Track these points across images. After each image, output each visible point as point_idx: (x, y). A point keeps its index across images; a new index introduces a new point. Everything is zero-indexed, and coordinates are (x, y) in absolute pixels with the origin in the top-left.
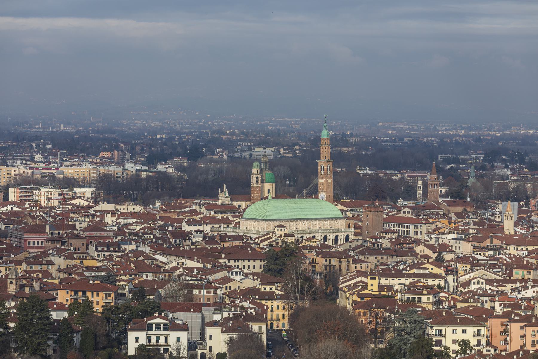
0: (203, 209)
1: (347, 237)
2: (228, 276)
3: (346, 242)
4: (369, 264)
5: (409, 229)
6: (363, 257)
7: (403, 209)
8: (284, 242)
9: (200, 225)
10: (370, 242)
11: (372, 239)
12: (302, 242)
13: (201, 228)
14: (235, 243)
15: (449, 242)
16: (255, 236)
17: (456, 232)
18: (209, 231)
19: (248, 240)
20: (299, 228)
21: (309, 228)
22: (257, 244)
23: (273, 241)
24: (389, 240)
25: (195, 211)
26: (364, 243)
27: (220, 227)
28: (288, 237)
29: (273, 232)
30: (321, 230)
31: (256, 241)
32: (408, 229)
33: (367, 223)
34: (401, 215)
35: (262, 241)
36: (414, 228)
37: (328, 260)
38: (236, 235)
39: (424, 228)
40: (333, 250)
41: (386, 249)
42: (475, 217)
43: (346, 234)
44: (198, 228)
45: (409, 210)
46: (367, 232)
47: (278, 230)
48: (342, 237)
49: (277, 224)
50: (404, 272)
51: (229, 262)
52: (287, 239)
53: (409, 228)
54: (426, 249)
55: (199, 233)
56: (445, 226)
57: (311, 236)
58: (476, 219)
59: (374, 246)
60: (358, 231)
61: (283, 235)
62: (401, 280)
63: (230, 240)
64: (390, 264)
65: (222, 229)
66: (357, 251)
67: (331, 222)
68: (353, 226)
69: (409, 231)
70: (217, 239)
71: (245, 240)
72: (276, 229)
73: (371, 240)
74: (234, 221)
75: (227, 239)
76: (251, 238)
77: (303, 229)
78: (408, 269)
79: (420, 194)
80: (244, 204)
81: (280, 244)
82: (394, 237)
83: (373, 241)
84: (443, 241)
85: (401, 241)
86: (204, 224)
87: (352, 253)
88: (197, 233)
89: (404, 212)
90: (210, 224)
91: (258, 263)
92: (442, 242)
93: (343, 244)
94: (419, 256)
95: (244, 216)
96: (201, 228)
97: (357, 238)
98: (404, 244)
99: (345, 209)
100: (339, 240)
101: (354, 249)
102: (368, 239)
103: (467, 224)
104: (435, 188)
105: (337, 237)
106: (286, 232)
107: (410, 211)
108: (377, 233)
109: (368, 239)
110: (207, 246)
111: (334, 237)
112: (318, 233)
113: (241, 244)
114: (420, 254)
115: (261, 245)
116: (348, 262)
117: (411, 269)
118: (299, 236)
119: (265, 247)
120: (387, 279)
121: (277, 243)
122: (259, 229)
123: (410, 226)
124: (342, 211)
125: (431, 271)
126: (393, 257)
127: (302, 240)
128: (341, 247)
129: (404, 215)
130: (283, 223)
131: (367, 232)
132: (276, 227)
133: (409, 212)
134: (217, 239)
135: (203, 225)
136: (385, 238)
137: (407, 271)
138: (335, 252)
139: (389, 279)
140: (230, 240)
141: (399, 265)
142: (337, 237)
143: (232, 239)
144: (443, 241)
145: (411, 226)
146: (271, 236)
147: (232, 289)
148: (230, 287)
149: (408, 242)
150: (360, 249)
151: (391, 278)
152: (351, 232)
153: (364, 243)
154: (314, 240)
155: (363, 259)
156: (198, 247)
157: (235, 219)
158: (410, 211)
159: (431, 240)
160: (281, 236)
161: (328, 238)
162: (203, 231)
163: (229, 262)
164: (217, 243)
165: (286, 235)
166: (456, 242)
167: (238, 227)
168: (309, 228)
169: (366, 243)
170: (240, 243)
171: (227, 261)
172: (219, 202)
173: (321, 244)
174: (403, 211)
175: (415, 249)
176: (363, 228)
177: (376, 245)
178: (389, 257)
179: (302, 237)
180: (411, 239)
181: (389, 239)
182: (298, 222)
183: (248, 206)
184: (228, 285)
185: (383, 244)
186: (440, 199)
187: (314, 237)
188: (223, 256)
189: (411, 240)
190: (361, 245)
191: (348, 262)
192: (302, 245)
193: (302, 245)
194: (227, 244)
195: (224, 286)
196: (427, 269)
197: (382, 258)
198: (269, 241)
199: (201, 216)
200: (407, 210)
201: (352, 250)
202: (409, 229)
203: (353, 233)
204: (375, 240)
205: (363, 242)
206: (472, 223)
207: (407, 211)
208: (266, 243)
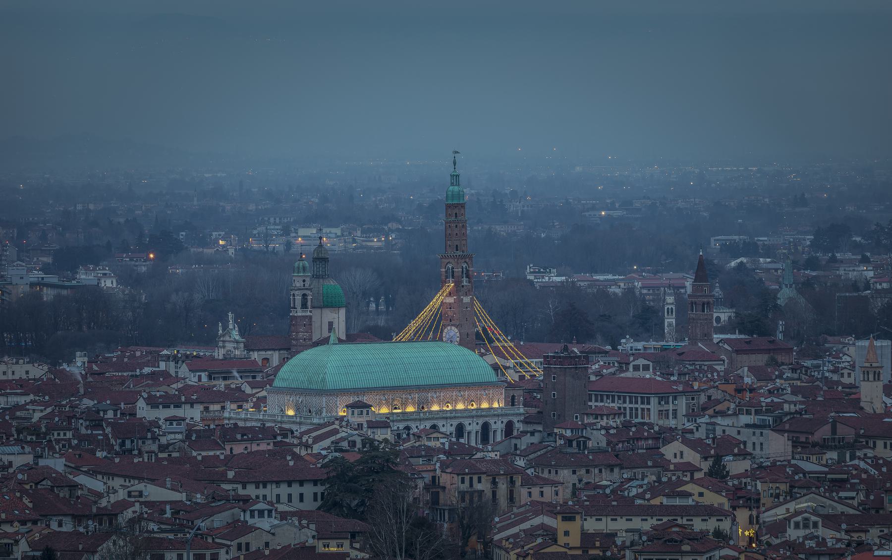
0: (184, 371)
2: (242, 519)
4: (560, 488)
5: (648, 407)
6: (546, 471)
7: (634, 361)
8: (369, 442)
9: (178, 406)
10: (562, 436)
11: (566, 429)
13: (179, 412)
15: (739, 433)
16: (304, 428)
17: (753, 410)
18: (197, 416)
19: (285, 436)
22: (307, 446)
23: (343, 439)
24: (603, 432)
25: (166, 374)
27: (223, 408)
28: (375, 430)
31: (304, 440)
32: (645, 406)
33: (554, 394)
34: (630, 374)
35: (317, 440)
36: (659, 403)
37: (467, 478)
38: (259, 427)
39: (682, 404)
40: (479, 455)
41: (599, 451)
42: (796, 376)
43: (505, 420)
44: (172, 412)
45: (646, 362)
46: (554, 414)
48: (498, 426)
49: (351, 400)
50: (639, 502)
51: (244, 488)
53: (649, 403)
54: (687, 451)
55: (175, 423)
56: (728, 397)
57: (428, 424)
58: (799, 379)
59: (571, 445)
61: (365, 425)
62: (631, 520)
64: (607, 486)
65: (226, 415)
66: (532, 456)
69: (649, 410)
71: (279, 438)
74: (253, 395)
75: (239, 437)
76: (292, 432)
78: (648, 496)
80: (275, 358)
81: (359, 445)
82: (614, 425)
83: (568, 433)
84: (724, 431)
85: (631, 433)
86: (185, 403)
87: (521, 463)
88: (171, 424)
89: (636, 368)
90: (202, 403)
91: (309, 490)
92: (721, 434)
93: (500, 443)
94: (672, 467)
95: (277, 383)
96: (179, 412)
97: (530, 428)
98: (638, 439)
100: (491, 435)
101: (523, 455)
102: (556, 430)
103: (778, 390)
104: (703, 311)
105: (486, 427)
108: (577, 416)
109: (556, 430)
110: (194, 454)
111: (479, 428)
113: (271, 447)
114: (674, 461)
115: (316, 449)
117: (652, 498)
118: (401, 426)
119: (324, 453)
120: (601, 520)
123: (648, 398)
125: (700, 500)
126: (612, 470)
127: (408, 435)
129: (637, 374)
130: (366, 399)
131: (554, 414)
133: (646, 368)
135: (183, 405)
137: (645, 499)
139: (604, 519)
140: (245, 437)
141: (626, 486)
142: (486, 427)
143: (250, 436)
144: (724, 431)
145: (652, 400)
146: (338, 427)
147: (253, 548)
148: (247, 544)
149: (646, 434)
150: (539, 453)
151: (609, 518)
154: (435, 435)
155: (546, 475)
156: (175, 455)
157: (255, 391)
159: (697, 430)
160: (360, 426)
161: (468, 428)
162: (184, 419)
163: (244, 488)
164: (217, 446)
166: (754, 434)
169: (552, 439)
171: (240, 487)
172: (219, 354)
173: (451, 444)
175: (662, 450)
177: (574, 444)
178: (603, 470)
179: (408, 428)
180: (653, 428)
181: (602, 428)
183: (284, 361)
184: (243, 540)
185: (589, 439)
186: (715, 336)
187: (434, 427)
188: (231, 474)
189: (652, 431)
191: (512, 482)
192: (407, 445)
193: (407, 445)
194: (238, 449)
195: (234, 543)
196: (690, 495)
197: (588, 472)
198: (333, 438)
200: (641, 362)
202: (648, 407)
204: (572, 432)
206: (789, 389)
208: (327, 443)
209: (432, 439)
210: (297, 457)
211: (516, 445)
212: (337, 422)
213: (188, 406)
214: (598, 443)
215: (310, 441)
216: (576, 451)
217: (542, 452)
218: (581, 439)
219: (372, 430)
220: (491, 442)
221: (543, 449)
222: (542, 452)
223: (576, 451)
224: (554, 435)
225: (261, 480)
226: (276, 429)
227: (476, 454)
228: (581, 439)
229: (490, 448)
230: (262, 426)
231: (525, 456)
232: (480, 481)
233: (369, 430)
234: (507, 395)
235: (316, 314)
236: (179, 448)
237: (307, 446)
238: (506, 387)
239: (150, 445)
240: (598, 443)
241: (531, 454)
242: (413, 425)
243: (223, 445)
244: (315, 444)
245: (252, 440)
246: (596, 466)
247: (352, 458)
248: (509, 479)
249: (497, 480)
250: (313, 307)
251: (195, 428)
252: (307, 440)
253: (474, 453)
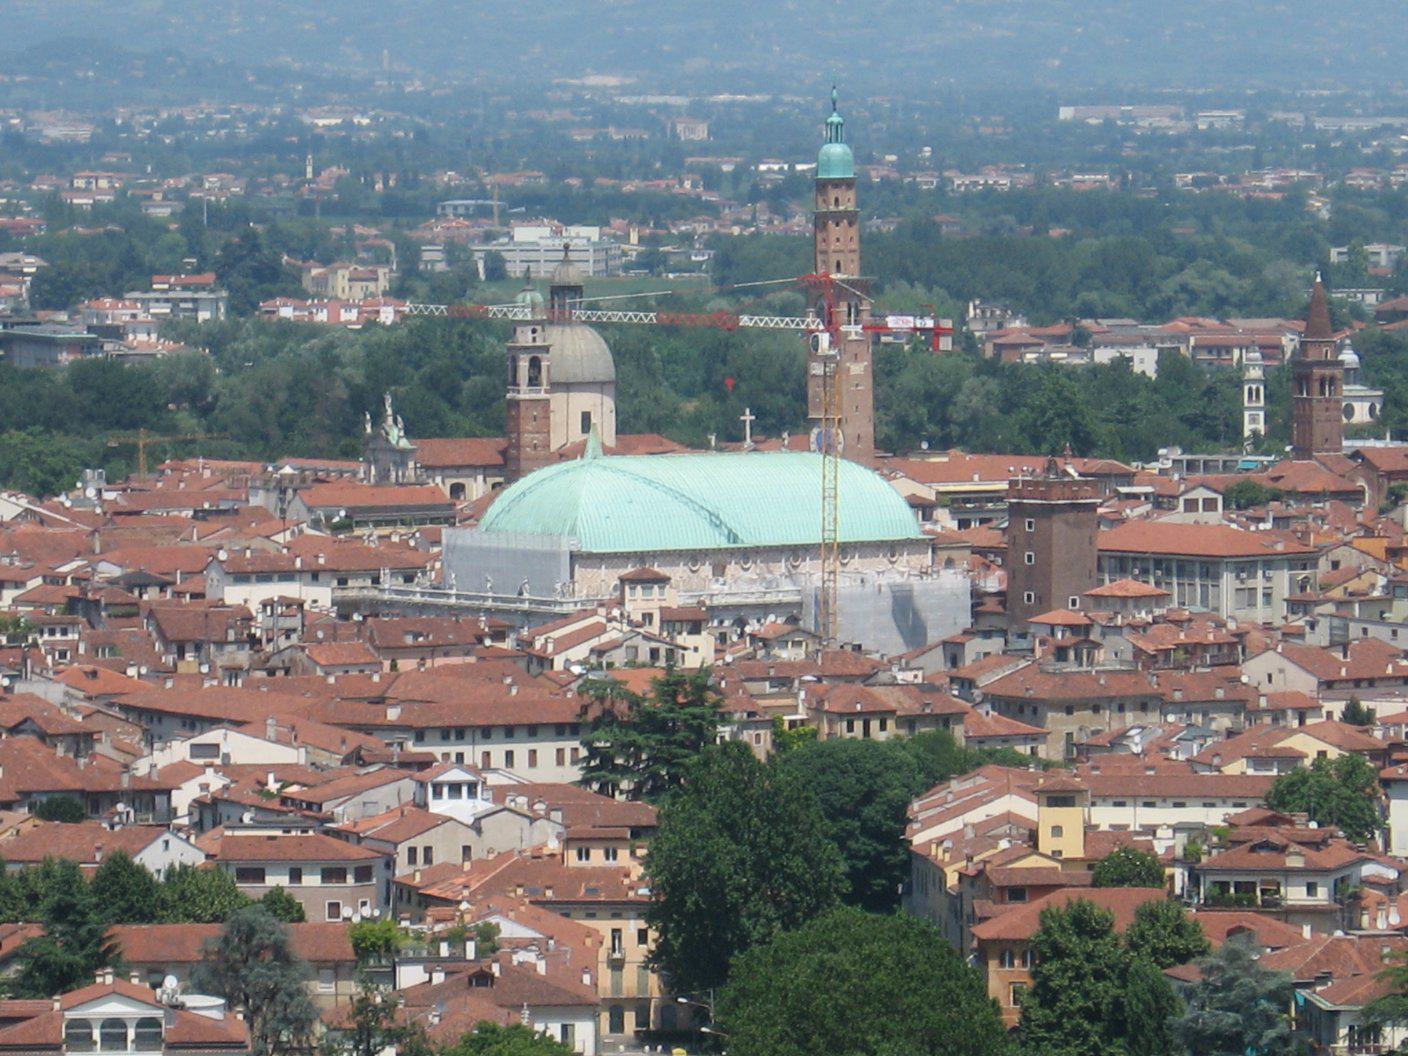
7: (1186, 492)
23: (615, 645)
33: (1030, 557)
45: (1211, 495)
46: (1029, 597)
79: (205, 787)
89: (1191, 506)
107: (1215, 501)
131: (1029, 597)
146: (604, 621)
148: (428, 850)
158: (1215, 501)
174: (1186, 501)
184: (420, 843)
198: (594, 642)
200: (1201, 494)
207: (1204, 500)
208: (580, 652)
212: (602, 611)
224: (1029, 637)
232: (883, 727)
235: (558, 400)
239: (231, 653)
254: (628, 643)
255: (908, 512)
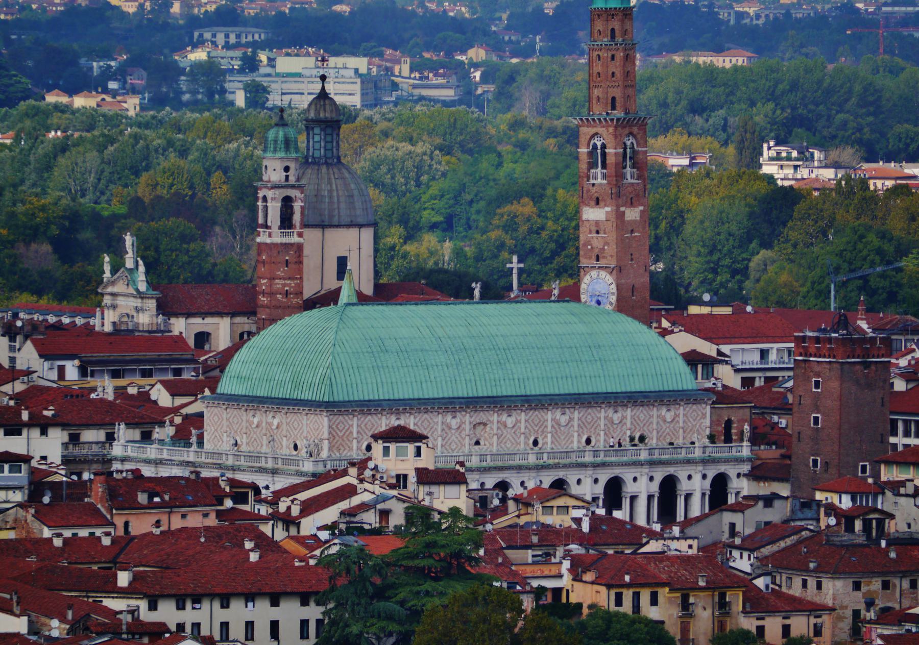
1: (720, 484)
3: (711, 508)
6: (797, 581)
10: (831, 509)
11: (840, 493)
12: (502, 510)
14: (184, 516)
16: (280, 483)
18: (55, 455)
19: (240, 498)
20: (491, 445)
21: (535, 443)
22: (288, 521)
26: (800, 515)
27: (111, 437)
28: (434, 488)
29: (362, 465)
30: (596, 453)
31: (282, 507)
33: (816, 419)
35: (310, 508)
37: (628, 595)
40: (653, 546)
43: (711, 474)
46: (815, 462)
47: (386, 451)
49: (385, 423)
51: (153, 607)
52: (430, 494)
57: (547, 480)
59: (850, 528)
60: (770, 453)
61: (412, 479)
63: (157, 499)
65: (117, 450)
66: (766, 551)
67: (641, 413)
68: (747, 435)
70: (97, 496)
71: (228, 503)
72: (378, 447)
73: (834, 498)
74: (175, 410)
75: (142, 498)
76: (257, 491)
77: (509, 447)
81: (397, 519)
83: (846, 503)
86: (30, 425)
87: (742, 563)
90: (64, 426)
93: (698, 520)
95: (226, 386)
97: (764, 489)
99: (708, 348)
101: (750, 545)
102: (819, 496)
105: (669, 486)
106: (427, 461)
109: (819, 496)
110: (47, 533)
111: (655, 488)
112: (583, 466)
115: (309, 525)
116: (723, 605)
118: (491, 481)
119: (324, 535)
121: (385, 514)
122: (296, 447)
124: (693, 359)
127: (504, 500)
128: (690, 531)
130: (411, 422)
131: (815, 462)
132: (376, 437)
134: (97, 496)
135: (25, 432)
136: (902, 491)
138: (659, 556)
140: (157, 499)
142: (669, 486)
143: (167, 497)
146: (355, 482)
150: (782, 544)
152: (739, 460)
153: (800, 515)
154: (561, 502)
155: (796, 590)
157: (179, 401)
160: (401, 480)
161: (630, 488)
162: (27, 459)
163: (153, 607)
164: (95, 518)
165: (426, 477)
167: (194, 439)
168: (535, 443)
169: (809, 513)
170: (206, 515)
171: (143, 605)
172: (106, 322)
173: (594, 518)
176: (794, 439)
177: (858, 525)
179: (503, 486)
182: (482, 416)
183: (241, 339)
185: (892, 517)
187: (559, 486)
188: (124, 579)
190: (786, 522)
191: (723, 605)
192: (502, 522)
193: (502, 522)
194: (142, 525)
197: (886, 585)
198: (344, 505)
199: (19, 386)
201: (740, 548)
203: (746, 468)
204: (853, 499)
205: (793, 511)
208: (330, 514)
209: (555, 509)
210: (265, 544)
211: (732, 526)
212: (353, 471)
213: (35, 433)
214: (909, 526)
215: (295, 511)
216: (862, 540)
217: (789, 541)
218: (871, 516)
219: (427, 489)
220: (680, 517)
221: (789, 536)
222: (789, 541)
223: (862, 540)
224: (814, 507)
225: (189, 591)
226: (222, 484)
227: (648, 542)
228: (871, 516)
229: (676, 530)
230: (193, 477)
231: (752, 550)
232: (654, 601)
233: (421, 488)
234: (715, 418)
235: (311, 239)
236: (16, 520)
237: (288, 521)
238: (714, 403)
240: (909, 526)
241: (763, 546)
242: (514, 480)
243: (109, 517)
244: (304, 516)
245: (169, 506)
246: (903, 575)
247: (381, 548)
248: (717, 599)
249: (692, 600)
250: (305, 225)
251: (50, 479)
252: (289, 508)
253: (644, 540)
254: (379, 507)
255: (685, 369)
